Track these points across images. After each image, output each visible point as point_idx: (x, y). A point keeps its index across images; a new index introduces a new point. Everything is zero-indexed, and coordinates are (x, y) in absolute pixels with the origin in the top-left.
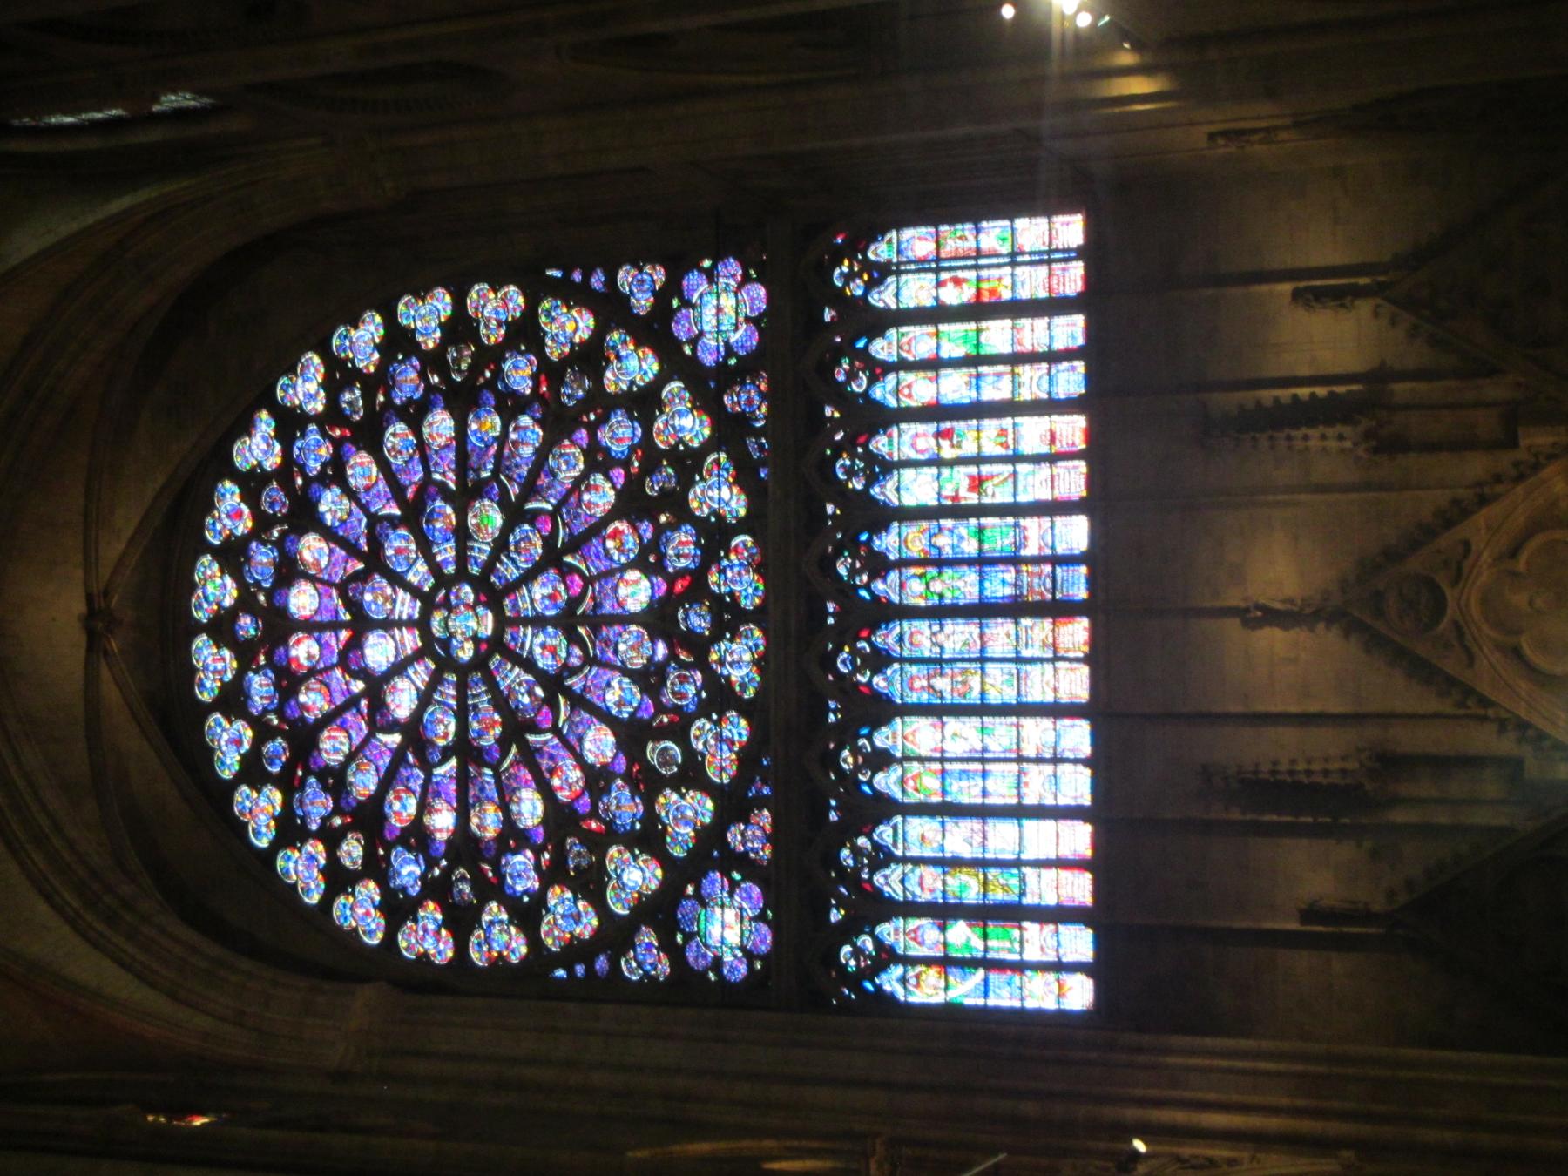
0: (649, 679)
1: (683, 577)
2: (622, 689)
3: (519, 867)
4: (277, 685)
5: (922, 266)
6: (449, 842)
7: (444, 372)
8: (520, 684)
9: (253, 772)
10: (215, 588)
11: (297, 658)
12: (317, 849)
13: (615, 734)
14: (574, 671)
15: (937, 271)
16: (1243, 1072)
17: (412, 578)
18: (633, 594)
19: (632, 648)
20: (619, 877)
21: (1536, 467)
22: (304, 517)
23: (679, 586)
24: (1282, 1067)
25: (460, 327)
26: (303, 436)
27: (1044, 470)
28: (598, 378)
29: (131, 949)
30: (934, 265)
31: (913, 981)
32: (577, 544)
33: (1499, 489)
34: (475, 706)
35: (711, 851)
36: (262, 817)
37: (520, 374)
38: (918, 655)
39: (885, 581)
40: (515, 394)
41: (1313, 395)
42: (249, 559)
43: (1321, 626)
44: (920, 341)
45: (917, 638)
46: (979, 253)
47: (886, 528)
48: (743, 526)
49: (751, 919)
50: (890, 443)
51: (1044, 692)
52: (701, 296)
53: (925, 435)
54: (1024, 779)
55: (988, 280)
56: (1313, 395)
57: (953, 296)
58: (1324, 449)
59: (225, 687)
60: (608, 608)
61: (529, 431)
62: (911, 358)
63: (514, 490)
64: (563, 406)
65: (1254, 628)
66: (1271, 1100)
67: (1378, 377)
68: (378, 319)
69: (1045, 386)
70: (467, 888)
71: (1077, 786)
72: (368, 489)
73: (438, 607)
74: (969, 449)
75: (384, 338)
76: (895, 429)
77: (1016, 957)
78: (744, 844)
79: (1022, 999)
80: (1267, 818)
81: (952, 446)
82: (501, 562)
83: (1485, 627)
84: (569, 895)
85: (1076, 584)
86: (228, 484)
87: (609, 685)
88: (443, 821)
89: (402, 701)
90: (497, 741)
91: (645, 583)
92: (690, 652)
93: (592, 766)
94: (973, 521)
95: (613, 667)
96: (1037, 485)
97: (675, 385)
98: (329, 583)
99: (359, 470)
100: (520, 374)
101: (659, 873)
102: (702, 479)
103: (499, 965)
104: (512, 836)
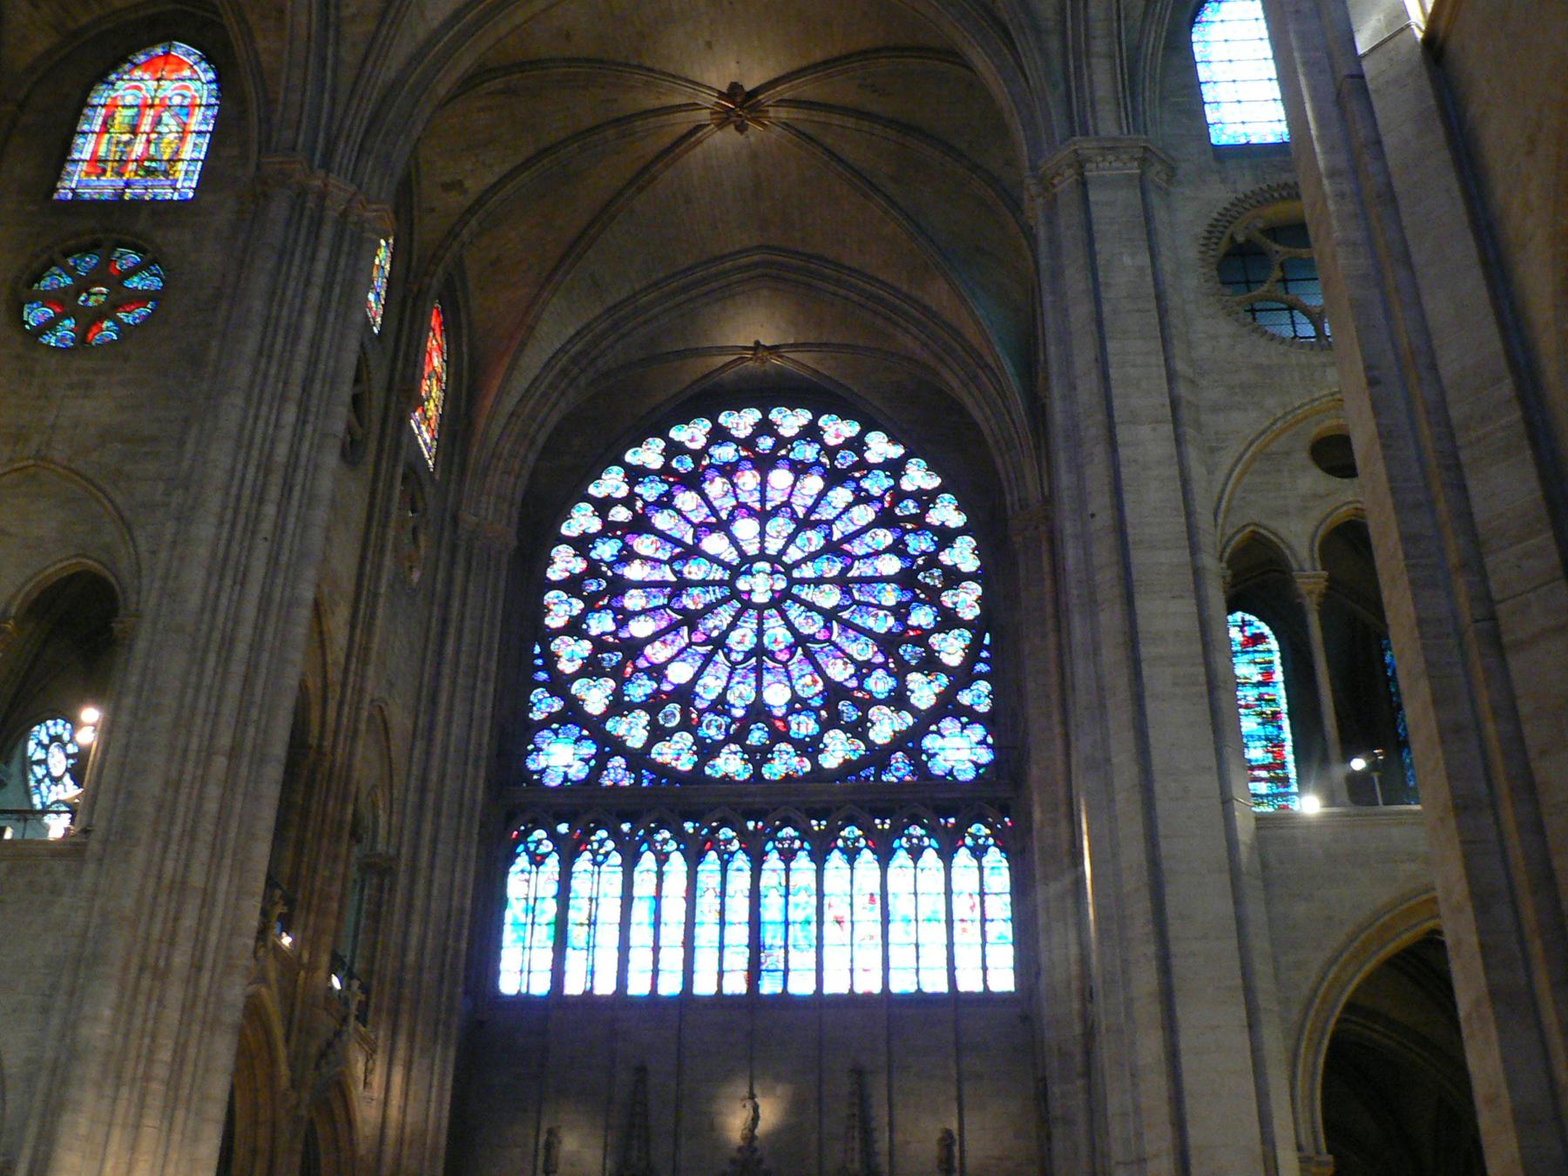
0: (720, 705)
4: (728, 463)
9: (674, 449)
12: (623, 491)
14: (727, 656)
22: (834, 478)
23: (779, 724)
25: (954, 577)
28: (918, 669)
29: (542, 388)
32: (810, 657)
35: (609, 746)
37: (922, 617)
49: (566, 774)
59: (727, 429)
60: (767, 678)
61: (883, 624)
63: (845, 615)
66: (409, 1111)
70: (594, 588)
72: (851, 520)
88: (634, 571)
89: (715, 544)
92: (736, 731)
94: (814, 918)
95: (728, 682)
97: (910, 720)
98: (790, 495)
100: (922, 617)
104: (624, 617)
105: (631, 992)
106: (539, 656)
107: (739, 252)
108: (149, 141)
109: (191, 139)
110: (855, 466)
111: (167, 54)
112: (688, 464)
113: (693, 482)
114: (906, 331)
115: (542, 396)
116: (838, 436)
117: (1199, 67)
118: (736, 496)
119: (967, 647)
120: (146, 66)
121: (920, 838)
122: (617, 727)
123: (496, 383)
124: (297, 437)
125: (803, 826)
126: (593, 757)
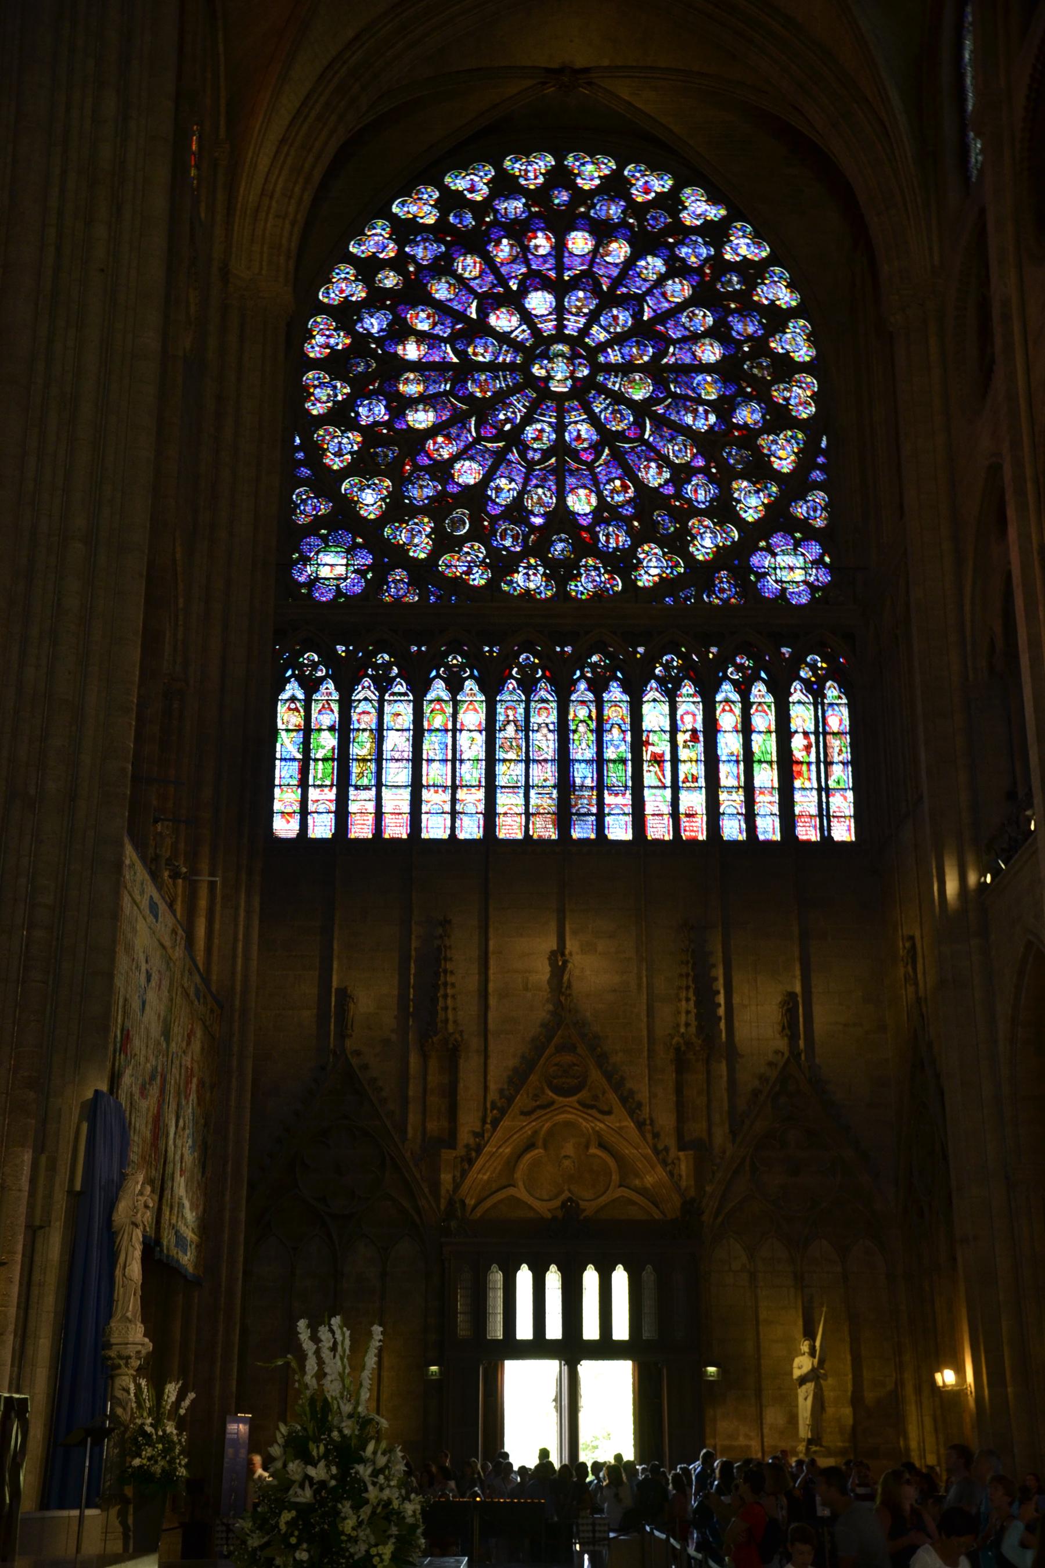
0: (517, 511)
1: (591, 538)
2: (509, 491)
3: (376, 409)
4: (516, 221)
5: (821, 721)
6: (396, 354)
7: (751, 356)
8: (514, 412)
9: (450, 201)
10: (591, 173)
11: (536, 237)
12: (391, 251)
13: (476, 484)
14: (523, 455)
15: (816, 733)
16: (234, 949)
17: (595, 329)
18: (580, 501)
19: (540, 498)
20: (369, 487)
21: (664, 1163)
24: (239, 977)
25: (786, 368)
26: (706, 244)
27: (666, 809)
30: (821, 731)
31: (293, 706)
32: (618, 458)
33: (649, 1136)
34: (497, 377)
35: (389, 556)
36: (415, 208)
37: (747, 415)
38: (532, 714)
39: (585, 690)
40: (732, 412)
41: (719, 1005)
42: (612, 199)
43: (550, 1007)
44: (763, 720)
45: (544, 714)
46: (829, 764)
47: (625, 692)
48: (630, 584)
49: (338, 586)
50: (689, 695)
51: (504, 805)
52: (803, 555)
53: (695, 721)
54: (440, 790)
55: (809, 770)
56: (719, 1005)
57: (798, 743)
58: (679, 1013)
60: (571, 481)
61: (704, 422)
62: (752, 711)
64: (723, 449)
65: (549, 959)
67: (732, 1053)
68: (794, 303)
69: (728, 811)
71: (435, 828)
72: (664, 294)
73: (572, 349)
74: (683, 754)
75: (779, 307)
76: (699, 699)
77: (311, 782)
78: (393, 581)
79: (280, 786)
80: (412, 965)
81: (685, 742)
82: (605, 400)
83: (548, 1125)
84: (356, 448)
86: (670, 182)
87: (511, 480)
89: (503, 321)
90: (472, 394)
91: (588, 510)
93: (452, 468)
94: (629, 756)
95: (525, 484)
96: (656, 804)
97: (736, 535)
98: (592, 263)
99: (680, 286)
100: (747, 415)
101: (372, 516)
102: (664, 554)
103: (304, 393)
104: (400, 405)
106: (298, 449)
110: (668, 230)
112: (469, 220)
116: (647, 192)
118: (527, 263)
119: (800, 450)
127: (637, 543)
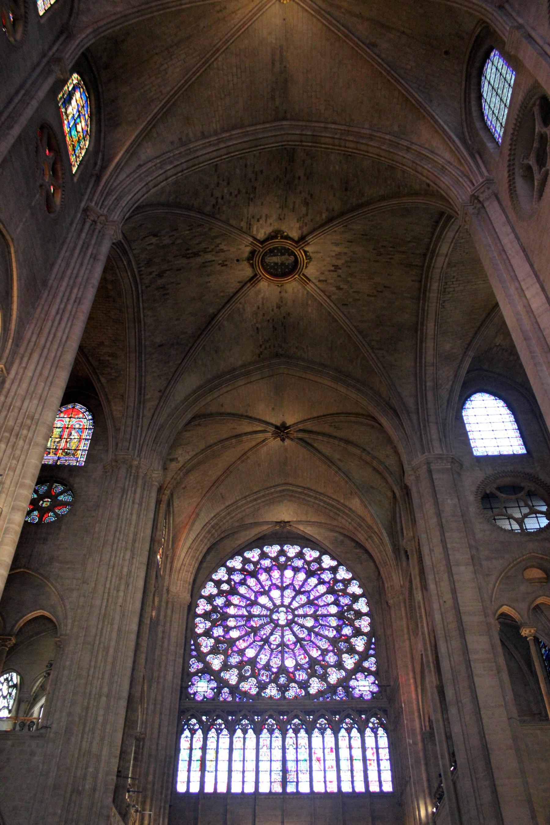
0: (267, 667)
4: (267, 567)
6: (227, 612)
9: (246, 561)
12: (226, 578)
14: (269, 646)
17: (294, 602)
22: (310, 574)
25: (359, 615)
28: (347, 652)
32: (302, 647)
35: (222, 683)
37: (347, 631)
48: (307, 693)
60: (286, 655)
61: (332, 634)
63: (317, 630)
70: (215, 617)
72: (317, 591)
77: (192, 769)
85: (291, 788)
88: (231, 611)
89: (263, 600)
92: (274, 678)
97: (344, 674)
98: (293, 580)
100: (347, 631)
104: (227, 629)
105: (233, 791)
107: (277, 485)
108: (66, 442)
109: (83, 442)
111: (73, 408)
112: (252, 567)
113: (254, 574)
114: (343, 518)
115: (201, 541)
117: (467, 425)
119: (366, 643)
120: (65, 412)
121: (351, 724)
122: (225, 675)
123: (184, 535)
124: (131, 564)
125: (304, 719)
126: (215, 688)
127: (310, 678)
